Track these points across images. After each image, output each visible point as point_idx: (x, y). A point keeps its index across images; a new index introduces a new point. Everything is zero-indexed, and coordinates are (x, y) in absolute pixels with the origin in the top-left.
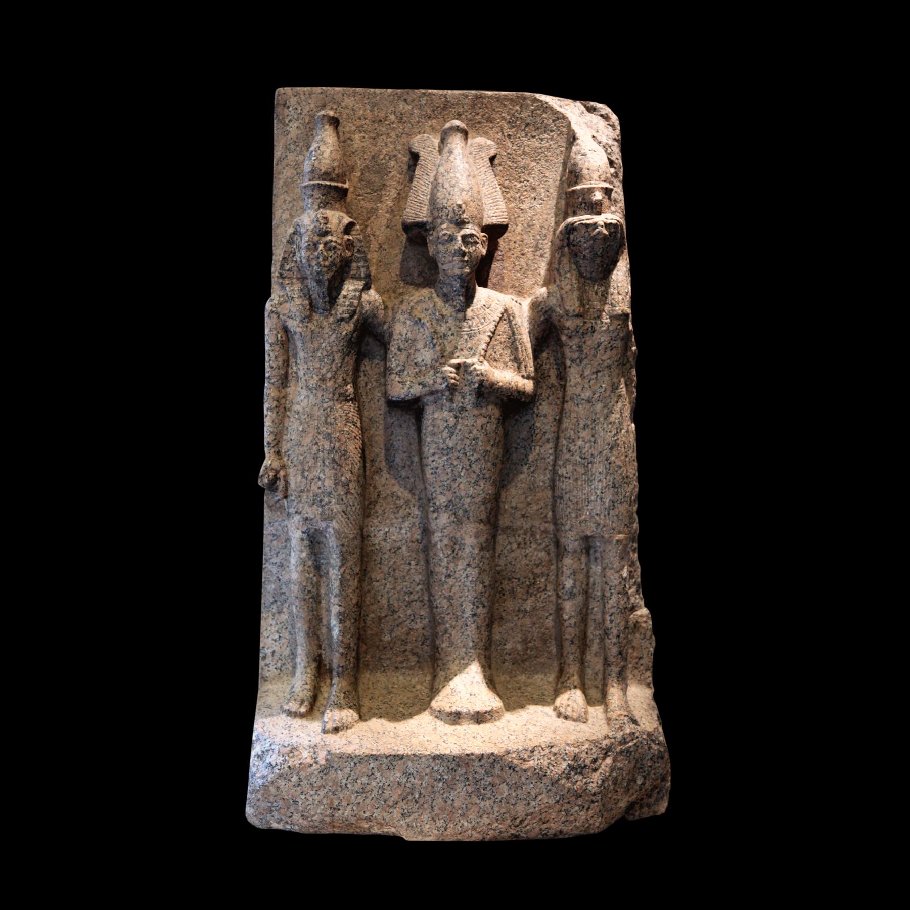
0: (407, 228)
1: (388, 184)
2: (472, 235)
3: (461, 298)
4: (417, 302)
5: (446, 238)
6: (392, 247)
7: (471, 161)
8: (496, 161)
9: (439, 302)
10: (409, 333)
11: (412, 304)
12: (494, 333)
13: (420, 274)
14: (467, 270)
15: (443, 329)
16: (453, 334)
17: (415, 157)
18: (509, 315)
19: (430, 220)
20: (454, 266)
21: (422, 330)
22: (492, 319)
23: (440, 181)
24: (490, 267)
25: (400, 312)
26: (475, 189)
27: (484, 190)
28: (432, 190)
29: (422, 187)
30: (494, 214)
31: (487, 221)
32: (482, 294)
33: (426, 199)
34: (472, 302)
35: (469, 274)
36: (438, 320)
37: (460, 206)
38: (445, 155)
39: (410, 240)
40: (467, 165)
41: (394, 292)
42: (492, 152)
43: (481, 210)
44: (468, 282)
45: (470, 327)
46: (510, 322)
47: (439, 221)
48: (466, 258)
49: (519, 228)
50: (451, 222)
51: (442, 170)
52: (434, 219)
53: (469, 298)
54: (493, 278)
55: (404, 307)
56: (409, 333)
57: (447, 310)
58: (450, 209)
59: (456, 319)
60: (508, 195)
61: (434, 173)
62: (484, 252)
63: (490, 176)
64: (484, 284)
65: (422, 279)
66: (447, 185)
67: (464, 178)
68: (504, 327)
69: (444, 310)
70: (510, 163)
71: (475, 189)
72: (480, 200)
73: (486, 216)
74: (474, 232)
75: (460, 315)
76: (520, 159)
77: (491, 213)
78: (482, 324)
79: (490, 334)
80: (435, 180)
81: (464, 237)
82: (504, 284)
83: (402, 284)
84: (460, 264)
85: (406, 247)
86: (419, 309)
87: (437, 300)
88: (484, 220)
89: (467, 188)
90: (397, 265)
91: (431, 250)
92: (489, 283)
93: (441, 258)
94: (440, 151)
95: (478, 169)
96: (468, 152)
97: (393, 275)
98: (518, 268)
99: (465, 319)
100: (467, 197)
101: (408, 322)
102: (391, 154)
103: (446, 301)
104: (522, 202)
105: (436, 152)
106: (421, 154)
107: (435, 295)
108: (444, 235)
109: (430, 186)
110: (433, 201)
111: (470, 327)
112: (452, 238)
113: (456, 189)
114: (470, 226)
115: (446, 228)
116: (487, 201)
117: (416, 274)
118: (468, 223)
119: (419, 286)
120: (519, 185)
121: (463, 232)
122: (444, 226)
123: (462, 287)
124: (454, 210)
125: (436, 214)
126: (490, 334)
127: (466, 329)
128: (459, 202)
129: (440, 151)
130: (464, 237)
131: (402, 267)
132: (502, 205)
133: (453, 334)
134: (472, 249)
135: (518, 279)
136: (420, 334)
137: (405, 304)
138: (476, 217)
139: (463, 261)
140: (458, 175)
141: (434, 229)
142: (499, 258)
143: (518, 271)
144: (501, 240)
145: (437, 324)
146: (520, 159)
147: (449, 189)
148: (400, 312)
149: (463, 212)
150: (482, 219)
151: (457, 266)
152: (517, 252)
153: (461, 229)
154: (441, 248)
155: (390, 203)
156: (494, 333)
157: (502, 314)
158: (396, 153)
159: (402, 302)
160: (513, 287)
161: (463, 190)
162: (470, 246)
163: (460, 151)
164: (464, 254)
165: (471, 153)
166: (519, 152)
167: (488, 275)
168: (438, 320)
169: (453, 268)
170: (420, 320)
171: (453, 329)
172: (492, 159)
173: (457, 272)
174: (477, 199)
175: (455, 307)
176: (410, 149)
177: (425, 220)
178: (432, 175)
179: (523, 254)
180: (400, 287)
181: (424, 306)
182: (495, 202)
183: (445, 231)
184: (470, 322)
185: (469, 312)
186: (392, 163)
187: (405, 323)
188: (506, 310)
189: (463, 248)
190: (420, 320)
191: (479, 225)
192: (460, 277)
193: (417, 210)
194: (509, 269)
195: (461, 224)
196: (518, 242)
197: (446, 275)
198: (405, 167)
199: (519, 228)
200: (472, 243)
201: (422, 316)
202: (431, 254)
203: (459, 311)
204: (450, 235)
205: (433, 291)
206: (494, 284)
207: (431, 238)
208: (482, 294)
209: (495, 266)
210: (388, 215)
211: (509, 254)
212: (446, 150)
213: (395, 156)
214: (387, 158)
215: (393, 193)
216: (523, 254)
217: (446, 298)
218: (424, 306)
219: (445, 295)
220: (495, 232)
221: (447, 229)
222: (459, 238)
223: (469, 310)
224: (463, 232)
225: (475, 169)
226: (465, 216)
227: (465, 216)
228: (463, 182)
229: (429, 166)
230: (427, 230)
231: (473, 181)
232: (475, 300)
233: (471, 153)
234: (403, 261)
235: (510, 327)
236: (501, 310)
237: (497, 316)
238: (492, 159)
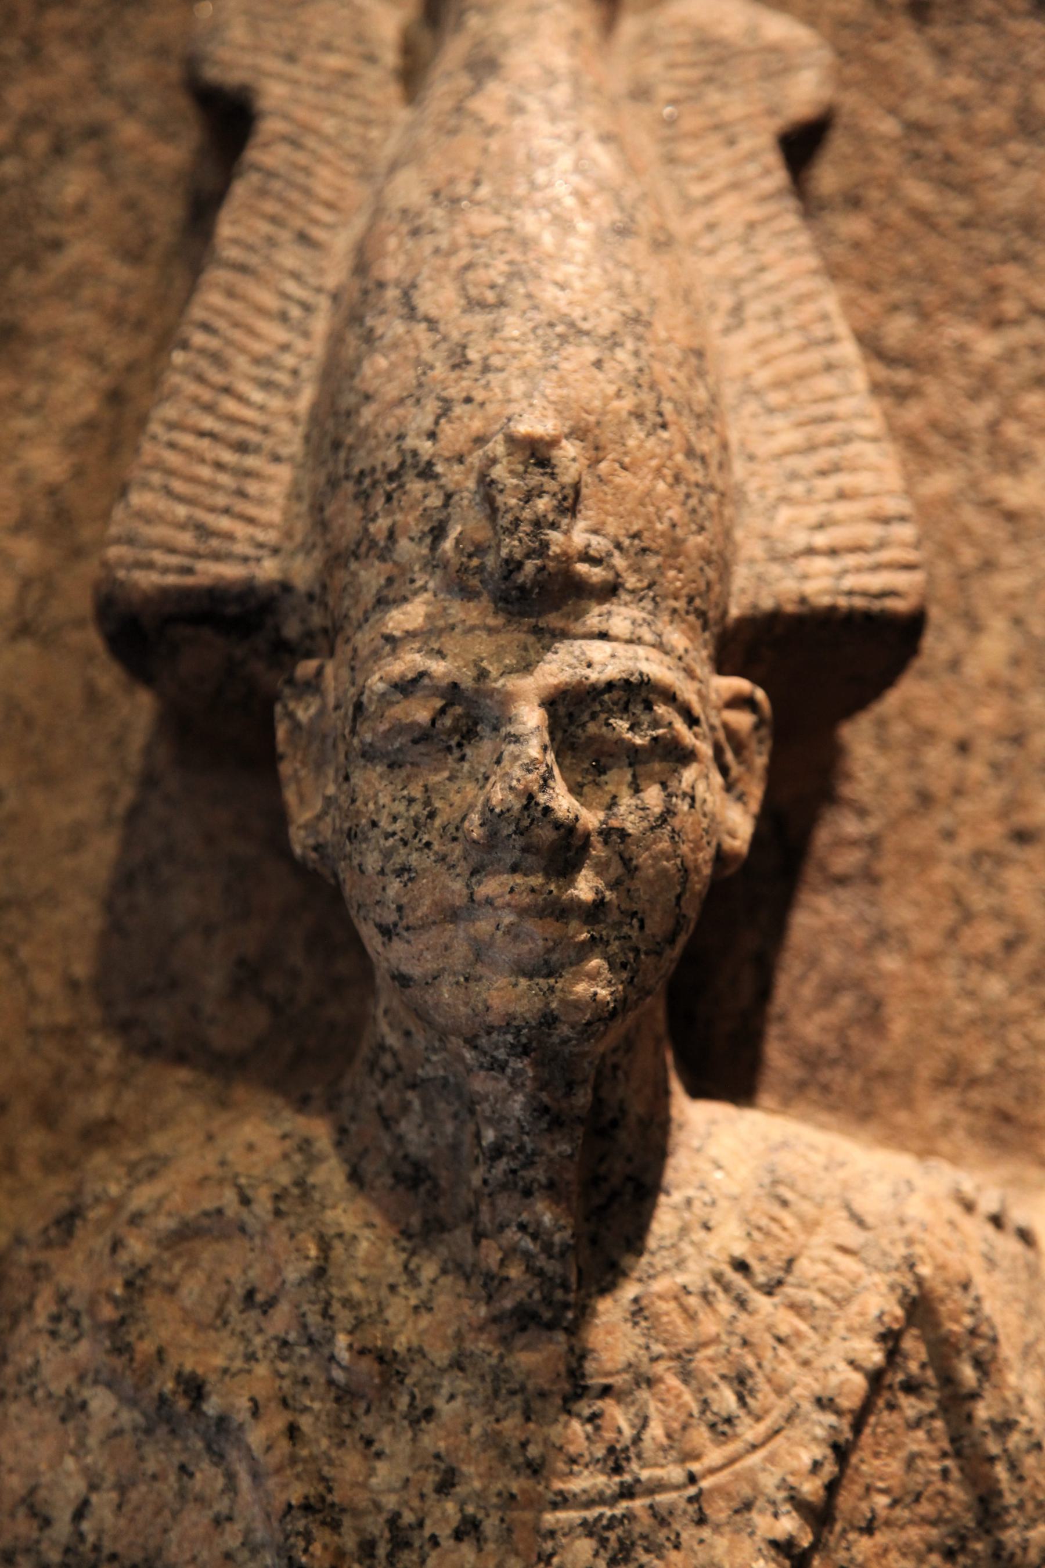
0: (143, 632)
1: (37, 321)
2: (636, 693)
3: (546, 1213)
4: (185, 1235)
5: (420, 712)
6: (48, 779)
7: (646, 145)
8: (828, 176)
9: (360, 1229)
10: (103, 1502)
11: (137, 1248)
12: (820, 1515)
13: (247, 977)
14: (594, 984)
15: (384, 1473)
16: (468, 1529)
17: (227, 120)
18: (943, 1350)
19: (303, 572)
20: (479, 951)
21: (207, 1477)
22: (806, 1386)
23: (391, 269)
24: (776, 930)
25: (44, 1306)
26: (669, 328)
27: (736, 353)
28: (336, 339)
29: (260, 339)
30: (818, 529)
31: (759, 584)
32: (724, 1155)
33: (280, 412)
34: (635, 1240)
35: (607, 1015)
36: (344, 1395)
37: (537, 453)
38: (443, 87)
39: (179, 726)
40: (603, 158)
41: (47, 1115)
42: (804, 92)
43: (712, 498)
44: (607, 1073)
45: (615, 1460)
46: (956, 1402)
47: (371, 576)
48: (585, 887)
49: (994, 648)
50: (461, 585)
51: (409, 189)
52: (338, 559)
53: (614, 1194)
54: (801, 1013)
55: (79, 1270)
56: (103, 1502)
57: (425, 1313)
58: (460, 478)
59: (500, 1386)
60: (913, 414)
61: (359, 223)
62: (739, 824)
63: (787, 255)
64: (731, 1077)
65: (259, 1019)
66: (439, 297)
67: (580, 244)
68: (904, 1450)
69: (396, 1310)
70: (920, 193)
71: (669, 328)
72: (707, 417)
73: (749, 547)
74: (656, 668)
75: (534, 1359)
76: (995, 164)
77: (793, 526)
78: (722, 1428)
79: (788, 1524)
80: (362, 264)
81: (569, 708)
82: (884, 1055)
83: (107, 1052)
84: (538, 935)
85: (149, 781)
86: (192, 1289)
87: (346, 1214)
88: (741, 577)
89: (606, 321)
90: (79, 914)
91: (307, 806)
92: (776, 1055)
93: (374, 885)
94: (412, 75)
95: (689, 205)
96: (618, 81)
97: (46, 983)
98: (988, 936)
99: (576, 1386)
100: (605, 383)
101: (101, 1402)
102: (71, 115)
103: (421, 1233)
104: (1014, 461)
105: (378, 85)
106: (273, 94)
107: (330, 1173)
108: (407, 686)
109: (320, 325)
110: (333, 428)
111: (615, 1460)
112: (467, 718)
113: (513, 325)
114: (621, 617)
115: (417, 637)
116: (761, 438)
117: (214, 981)
118: (610, 591)
119: (225, 1069)
120: (988, 347)
121: (558, 667)
122: (411, 615)
123: (549, 1117)
124: (487, 485)
125: (348, 519)
126: (788, 1524)
127: (586, 1481)
128: (536, 423)
129: (412, 75)
130: (569, 708)
131: (116, 929)
132: (878, 471)
133: (468, 1529)
134: (636, 806)
135: (993, 1023)
136: (195, 1520)
137: (91, 1240)
138: (675, 548)
139: (562, 911)
140: (530, 222)
141: (328, 638)
142: (846, 861)
143: (987, 962)
144: (858, 737)
145: (339, 1430)
146: (995, 164)
147: (459, 326)
148: (44, 1306)
149: (570, 504)
150: (720, 562)
151: (506, 952)
152: (979, 818)
153: (549, 637)
154: (379, 792)
155: (47, 461)
156: (820, 1515)
157: (890, 1340)
158: (103, 109)
159: (68, 1221)
160: (954, 1077)
161: (574, 332)
162: (618, 779)
163: (561, 60)
164: (567, 849)
165: (641, 93)
166: (992, 117)
167: (764, 992)
168: (344, 1395)
169: (470, 964)
170: (195, 1389)
171: (473, 1478)
172: (801, 145)
173: (507, 995)
174: (685, 410)
175: (492, 1284)
176: (192, 64)
177: (269, 569)
178: (341, 243)
179: (1022, 837)
180: (90, 1081)
181: (236, 1265)
182: (824, 444)
183: (410, 661)
184: (619, 1417)
185: (613, 1335)
186: (74, 184)
187: (74, 1409)
188: (919, 1307)
189: (562, 801)
190: (195, 1389)
191: (701, 611)
192: (537, 1040)
193: (220, 508)
194: (926, 940)
195: (542, 597)
196: (987, 748)
197: (421, 1014)
198: (167, 212)
199: (994, 648)
200: (634, 756)
201: (210, 1356)
202: (299, 841)
203: (525, 1321)
204: (453, 692)
205: (320, 1131)
206: (813, 1060)
207: (304, 713)
208: (724, 1155)
209: (819, 919)
210: (26, 550)
211: (920, 834)
212: (455, 50)
213: (95, 132)
214: (39, 142)
215: (75, 391)
216: (1022, 837)
217: (421, 1199)
218: (236, 1265)
219: (413, 1177)
220: (822, 667)
221: (429, 637)
222: (531, 717)
223: (611, 1311)
224: (558, 667)
225: (670, 201)
226: (579, 536)
227: (579, 536)
228: (573, 267)
229: (325, 180)
230: (286, 653)
231: (656, 276)
232: (664, 1222)
233: (641, 93)
234: (126, 879)
235: (962, 1446)
236: (879, 1302)
237: (841, 1363)
238: (801, 145)
